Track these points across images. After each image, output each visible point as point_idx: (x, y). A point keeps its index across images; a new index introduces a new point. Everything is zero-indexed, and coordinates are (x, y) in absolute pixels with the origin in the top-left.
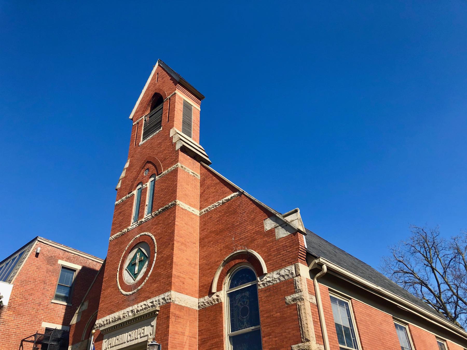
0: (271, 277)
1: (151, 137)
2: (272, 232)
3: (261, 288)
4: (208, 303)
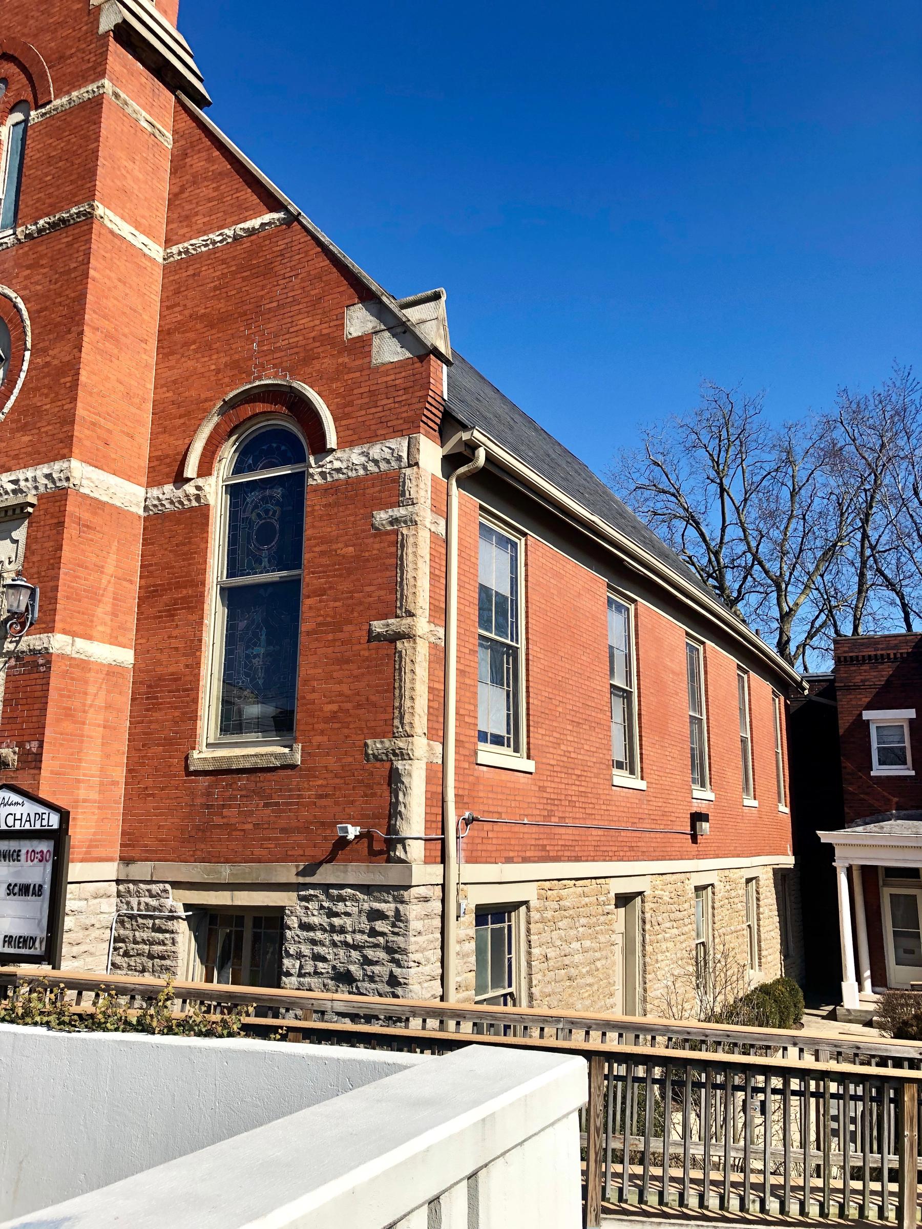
0: (344, 460)
2: (363, 344)
3: (314, 483)
4: (172, 503)
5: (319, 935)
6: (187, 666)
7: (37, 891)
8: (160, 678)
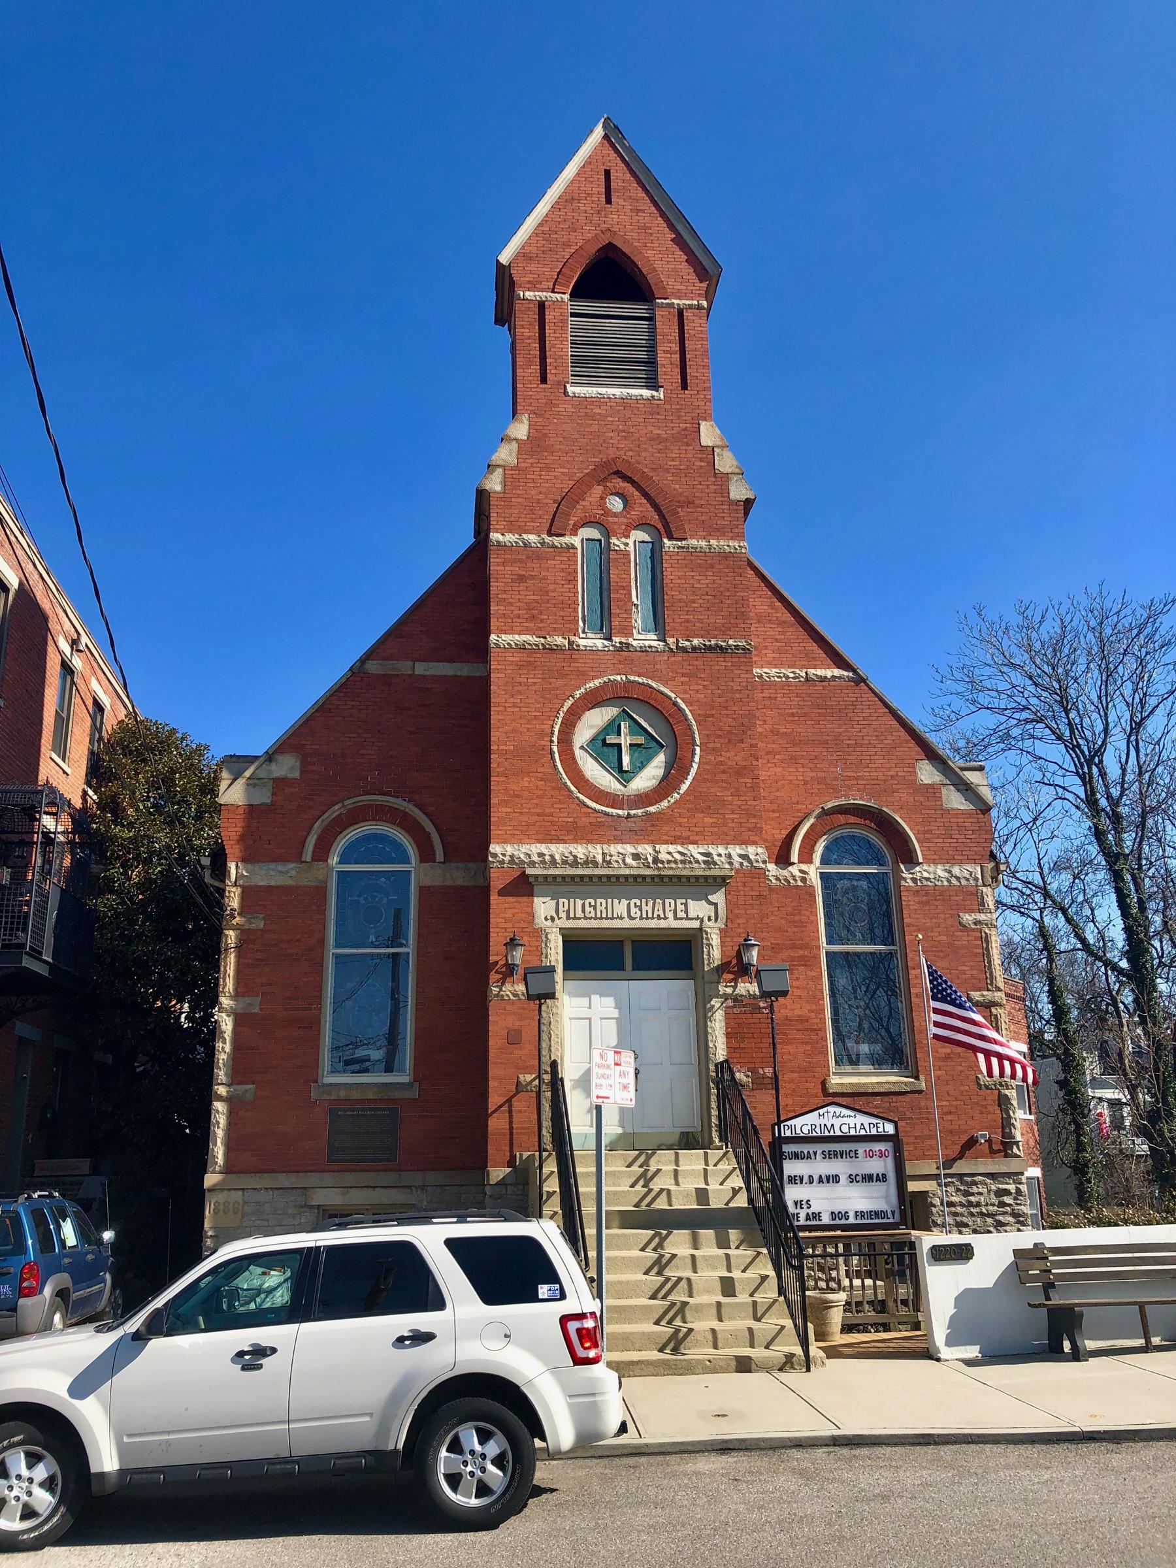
0: (930, 872)
1: (617, 392)
2: (932, 791)
4: (778, 879)
5: (959, 1209)
6: (811, 1011)
7: (882, 1178)
8: (787, 1019)
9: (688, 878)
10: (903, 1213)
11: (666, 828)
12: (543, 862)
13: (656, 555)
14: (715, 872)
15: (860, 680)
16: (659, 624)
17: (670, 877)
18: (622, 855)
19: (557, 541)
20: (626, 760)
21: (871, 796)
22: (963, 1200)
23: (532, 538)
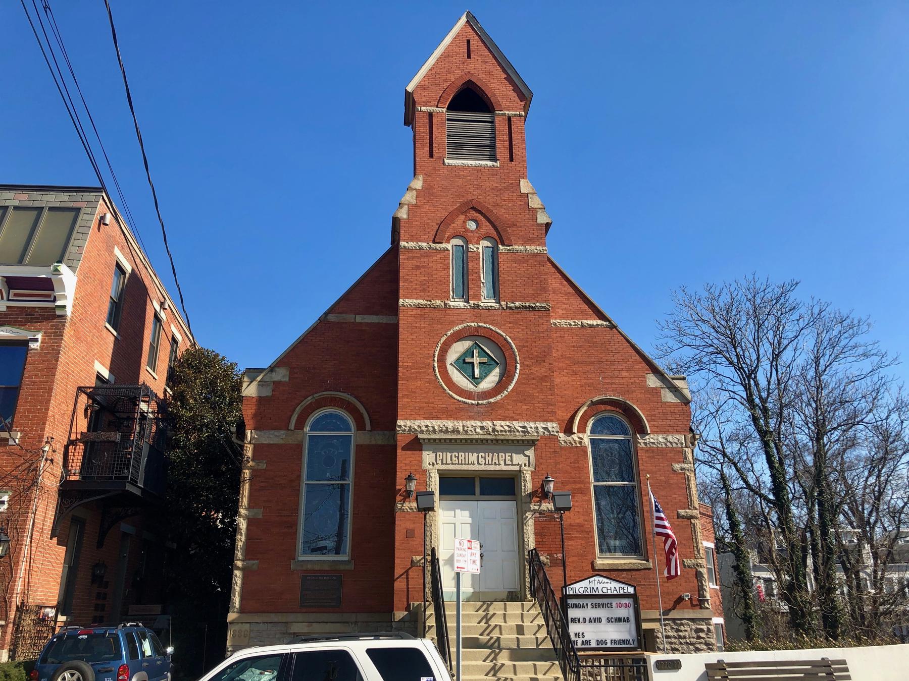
0: (654, 439)
2: (656, 391)
4: (565, 442)
5: (673, 640)
7: (627, 620)
8: (571, 525)
9: (513, 441)
10: (639, 641)
11: (499, 412)
12: (428, 431)
13: (494, 255)
14: (528, 438)
15: (613, 327)
16: (496, 294)
17: (502, 440)
18: (474, 427)
19: (438, 246)
20: (477, 371)
21: (619, 394)
22: (675, 634)
23: (424, 245)
